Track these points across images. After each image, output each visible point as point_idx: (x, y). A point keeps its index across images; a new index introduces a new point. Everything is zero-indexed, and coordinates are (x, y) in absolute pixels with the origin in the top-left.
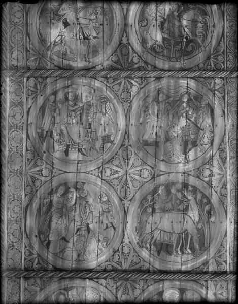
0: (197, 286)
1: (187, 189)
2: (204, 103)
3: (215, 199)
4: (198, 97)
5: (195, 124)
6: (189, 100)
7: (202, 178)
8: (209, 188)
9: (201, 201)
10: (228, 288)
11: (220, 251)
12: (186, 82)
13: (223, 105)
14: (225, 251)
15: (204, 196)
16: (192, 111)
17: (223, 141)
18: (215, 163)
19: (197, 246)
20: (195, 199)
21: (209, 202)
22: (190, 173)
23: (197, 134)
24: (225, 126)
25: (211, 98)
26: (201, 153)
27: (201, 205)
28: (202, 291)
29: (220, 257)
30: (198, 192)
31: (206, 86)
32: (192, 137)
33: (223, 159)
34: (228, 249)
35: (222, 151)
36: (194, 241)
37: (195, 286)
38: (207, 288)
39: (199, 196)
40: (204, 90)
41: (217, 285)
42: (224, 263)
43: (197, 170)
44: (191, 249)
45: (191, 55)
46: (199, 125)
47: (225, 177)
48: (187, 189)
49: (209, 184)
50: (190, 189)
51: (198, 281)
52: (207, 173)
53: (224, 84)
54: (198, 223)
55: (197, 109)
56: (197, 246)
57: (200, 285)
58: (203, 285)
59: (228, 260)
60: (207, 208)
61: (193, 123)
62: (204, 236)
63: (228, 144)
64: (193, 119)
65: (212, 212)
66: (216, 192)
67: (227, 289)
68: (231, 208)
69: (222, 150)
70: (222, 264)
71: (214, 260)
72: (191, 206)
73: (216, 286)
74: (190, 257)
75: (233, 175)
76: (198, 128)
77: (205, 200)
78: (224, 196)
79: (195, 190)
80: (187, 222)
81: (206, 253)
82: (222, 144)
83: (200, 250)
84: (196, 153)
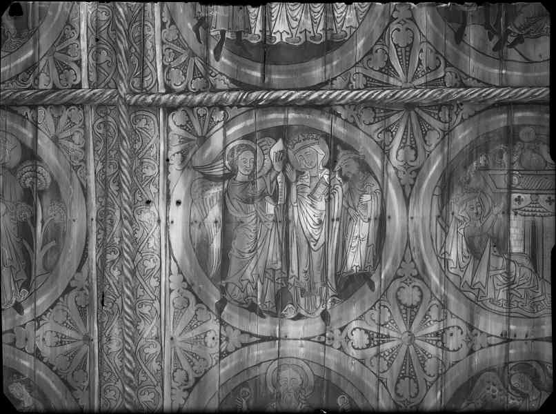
0: (12, 120)
10: (84, 124)
11: (64, 38)
14: (76, 36)
28: (24, 131)
29: (65, 51)
34: (83, 30)
37: (8, 123)
38: (35, 125)
41: (60, 117)
42: (74, 66)
51: (15, 109)
57: (20, 118)
58: (25, 118)
59: (84, 58)
67: (84, 126)
73: (56, 120)
81: (31, 42)
83: (19, 35)
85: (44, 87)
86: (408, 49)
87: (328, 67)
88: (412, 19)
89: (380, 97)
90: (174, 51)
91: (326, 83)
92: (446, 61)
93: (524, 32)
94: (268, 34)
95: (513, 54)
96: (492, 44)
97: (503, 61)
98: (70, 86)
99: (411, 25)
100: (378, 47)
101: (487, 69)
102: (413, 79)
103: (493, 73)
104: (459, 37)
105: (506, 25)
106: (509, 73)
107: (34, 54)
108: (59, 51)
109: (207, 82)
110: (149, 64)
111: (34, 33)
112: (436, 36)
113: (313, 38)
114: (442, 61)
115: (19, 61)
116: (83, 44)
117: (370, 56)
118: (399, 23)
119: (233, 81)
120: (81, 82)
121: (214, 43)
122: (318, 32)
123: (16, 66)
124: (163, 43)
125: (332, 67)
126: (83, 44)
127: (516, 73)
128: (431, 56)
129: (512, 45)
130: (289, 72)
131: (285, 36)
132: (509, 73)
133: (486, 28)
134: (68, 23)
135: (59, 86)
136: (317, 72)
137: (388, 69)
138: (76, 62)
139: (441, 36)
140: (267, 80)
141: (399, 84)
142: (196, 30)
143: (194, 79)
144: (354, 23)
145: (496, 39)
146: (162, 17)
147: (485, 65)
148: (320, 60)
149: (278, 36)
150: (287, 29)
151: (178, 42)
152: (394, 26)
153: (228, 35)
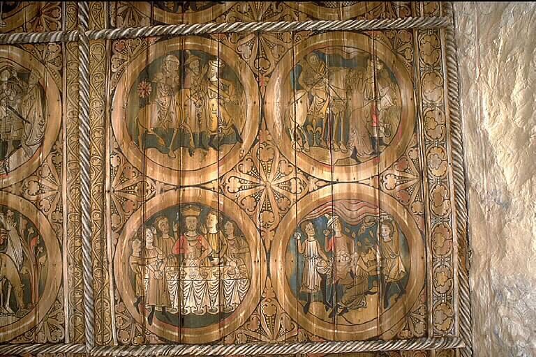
1: (5, 214)
2: (32, 82)
3: (45, 226)
4: (24, 75)
5: (19, 116)
6: (11, 79)
7: (26, 195)
8: (37, 211)
9: (26, 232)
12: (7, 51)
13: (60, 83)
14: (62, 308)
15: (30, 224)
16: (14, 96)
17: (58, 139)
18: (46, 172)
19: (20, 302)
20: (17, 228)
21: (37, 233)
22: (10, 189)
23: (22, 128)
24: (62, 115)
25: (42, 74)
26: (26, 159)
27: (26, 238)
30: (21, 218)
31: (37, 58)
32: (14, 134)
33: (58, 166)
34: (66, 304)
35: (56, 154)
36: (16, 293)
39: (22, 223)
40: (33, 63)
42: (60, 327)
43: (19, 184)
44: (11, 305)
45: (14, 11)
46: (24, 117)
47: (59, 193)
48: (5, 214)
49: (37, 204)
50: (10, 213)
52: (34, 188)
53: (61, 52)
54: (21, 266)
55: (22, 92)
56: (20, 302)
59: (67, 322)
60: (33, 244)
61: (16, 112)
62: (31, 289)
63: (65, 143)
64: (15, 108)
65: (41, 249)
66: (47, 217)
68: (69, 241)
69: (55, 152)
70: (58, 329)
71: (46, 322)
72: (11, 242)
74: (11, 319)
75: (71, 191)
76: (23, 121)
77: (31, 231)
78: (58, 222)
79: (16, 216)
80: (5, 266)
82: (57, 143)
84: (19, 158)
85: (42, 342)
86: (273, 317)
87: (222, 329)
88: (276, 298)
89: (254, 354)
90: (123, 319)
91: (221, 340)
92: (298, 325)
93: (349, 306)
94: (182, 308)
95: (341, 320)
96: (328, 313)
97: (334, 324)
98: (58, 340)
99: (274, 302)
100: (253, 316)
101: (325, 329)
102: (277, 338)
103: (330, 333)
104: (306, 309)
105: (337, 302)
106: (339, 332)
107: (35, 319)
108: (51, 317)
109: (144, 339)
110: (107, 327)
111: (36, 307)
112: (291, 310)
113: (211, 310)
114: (296, 325)
115: (25, 325)
116: (66, 312)
117: (248, 323)
118: (266, 301)
119: (160, 338)
120: (64, 338)
121: (148, 313)
122: (215, 306)
123: (23, 327)
124: (115, 313)
125: (224, 329)
126: (66, 312)
127: (343, 332)
128: (289, 322)
129: (340, 314)
130: (196, 333)
131: (193, 309)
132: (339, 332)
133: (324, 304)
134: (57, 299)
135: (50, 340)
136: (215, 333)
137: (260, 330)
138: (62, 325)
139: (294, 308)
140: (182, 337)
141: (268, 340)
142: (136, 305)
143: (136, 336)
144: (237, 301)
145: (330, 310)
146: (114, 296)
147: (324, 326)
148: (217, 325)
149: (188, 309)
150: (195, 305)
151: (125, 312)
152: (263, 303)
153: (156, 309)
